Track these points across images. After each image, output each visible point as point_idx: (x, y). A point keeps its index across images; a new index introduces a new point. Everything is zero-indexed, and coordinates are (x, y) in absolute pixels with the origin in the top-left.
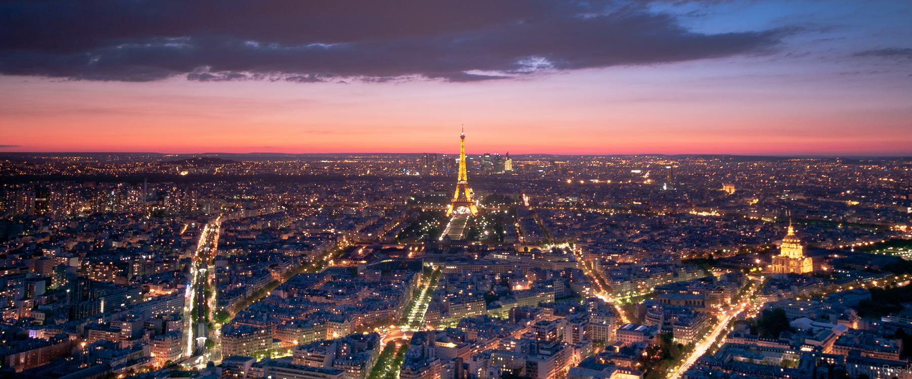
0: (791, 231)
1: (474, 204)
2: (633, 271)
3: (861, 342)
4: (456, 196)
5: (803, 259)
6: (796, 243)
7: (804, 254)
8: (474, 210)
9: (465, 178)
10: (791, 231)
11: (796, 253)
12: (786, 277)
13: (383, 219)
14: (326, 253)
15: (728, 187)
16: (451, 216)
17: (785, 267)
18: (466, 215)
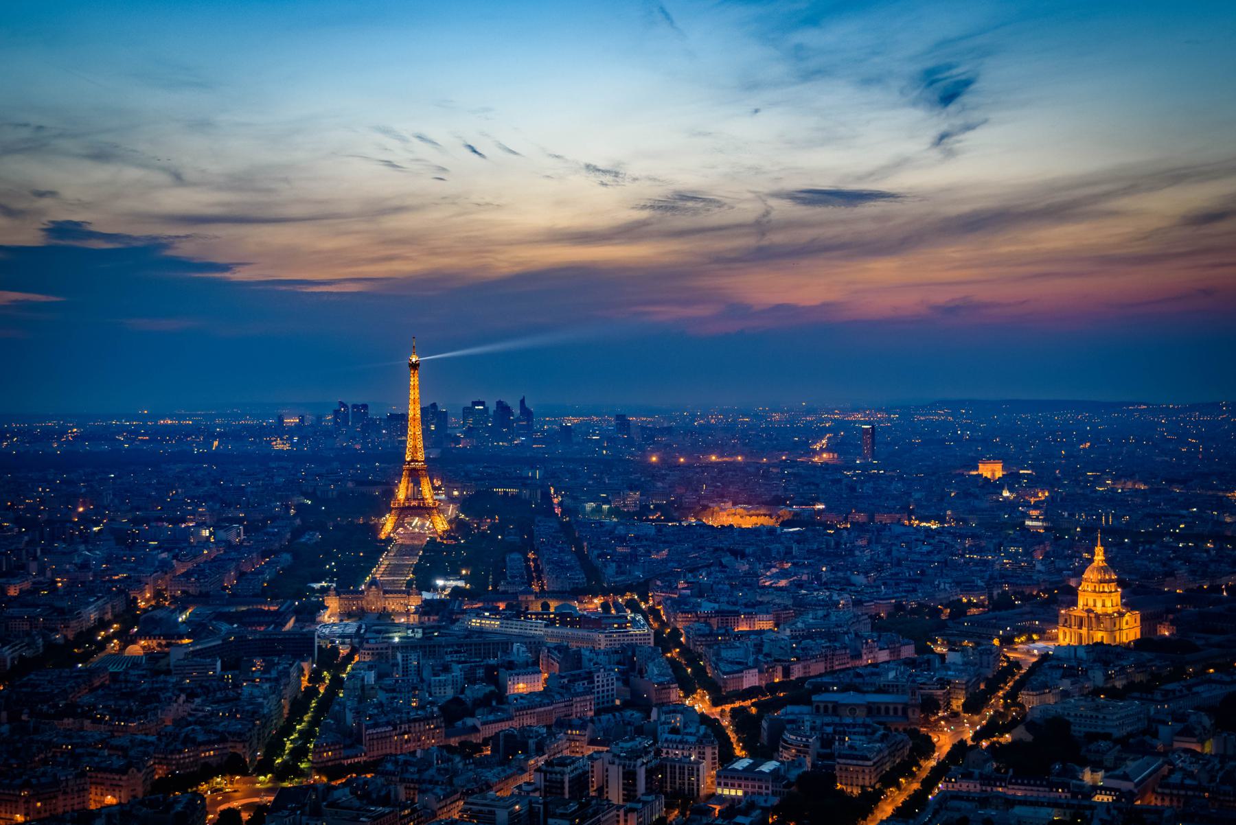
0: (1099, 556)
1: (440, 511)
2: (766, 650)
3: (1212, 779)
4: (402, 493)
5: (1121, 615)
6: (1110, 581)
7: (1124, 605)
8: (441, 524)
9: (421, 456)
10: (1099, 556)
11: (1108, 603)
12: (1082, 654)
13: (238, 548)
14: (103, 624)
15: (989, 466)
16: (389, 540)
17: (1084, 631)
18: (420, 536)
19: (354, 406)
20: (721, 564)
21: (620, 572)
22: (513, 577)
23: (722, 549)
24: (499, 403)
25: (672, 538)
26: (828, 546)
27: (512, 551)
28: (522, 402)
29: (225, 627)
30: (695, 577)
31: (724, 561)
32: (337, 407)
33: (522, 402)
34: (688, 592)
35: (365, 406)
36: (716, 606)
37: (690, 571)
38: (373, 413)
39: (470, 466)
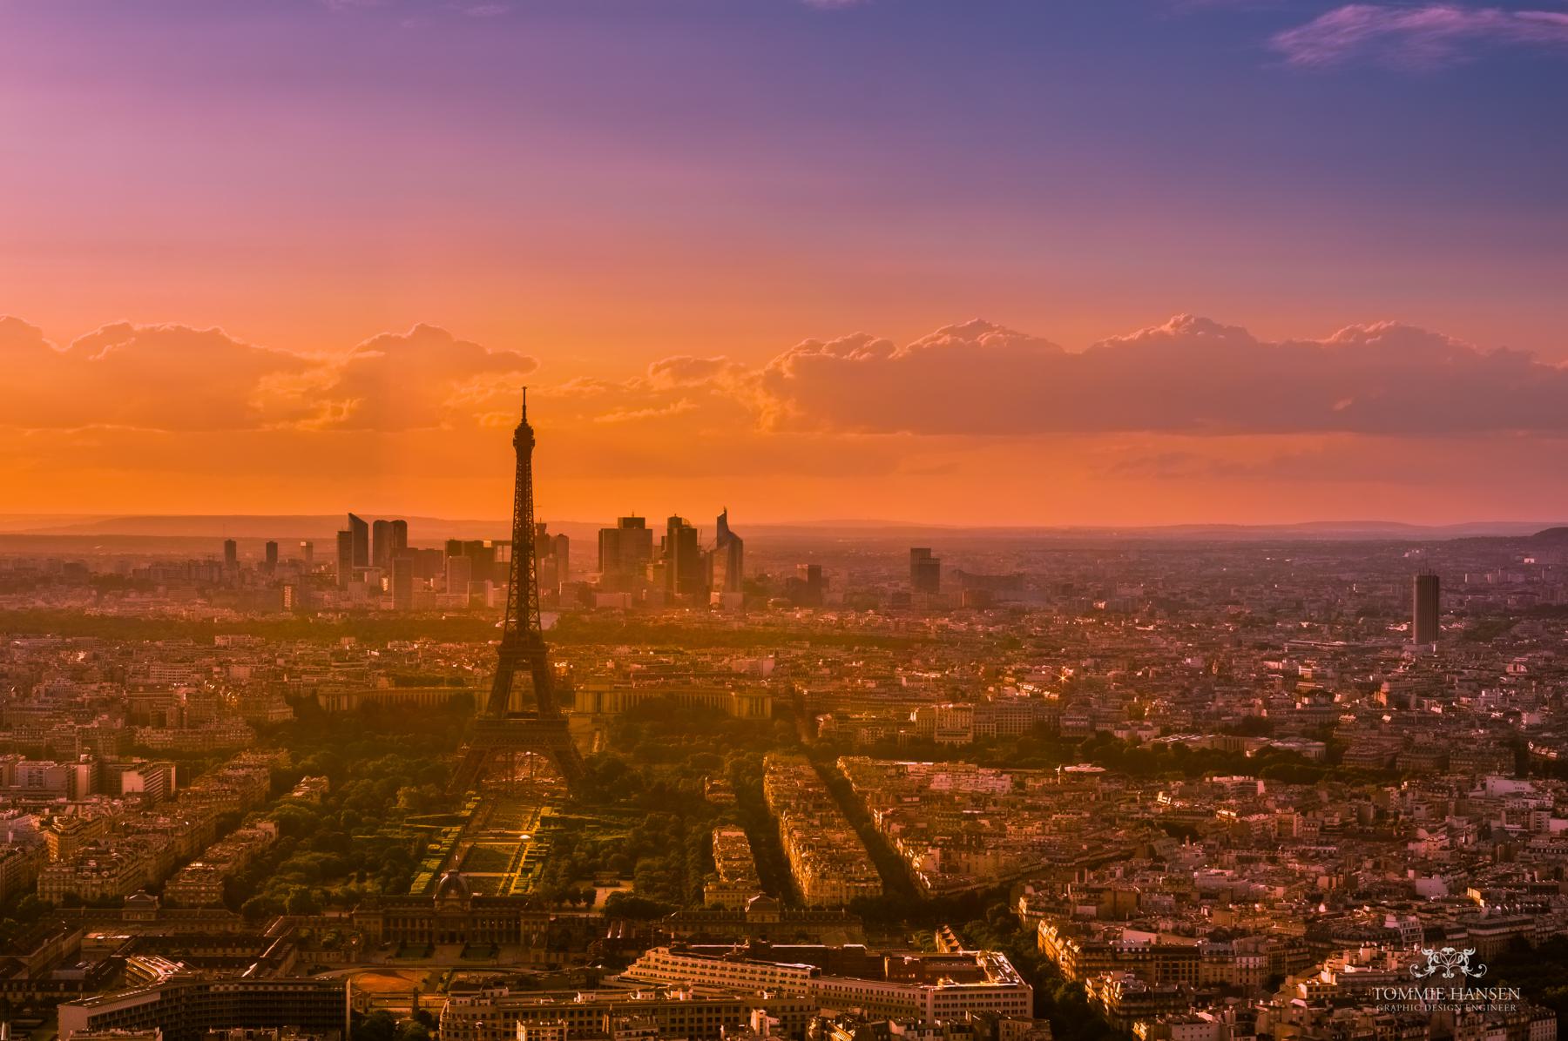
19: (380, 525)
20: (1151, 853)
21: (948, 866)
22: (731, 874)
23: (1150, 823)
24: (675, 522)
25: (1045, 801)
26: (1362, 819)
27: (724, 824)
28: (722, 520)
29: (162, 970)
30: (1101, 878)
31: (1159, 845)
32: (346, 527)
33: (722, 520)
34: (1092, 909)
35: (400, 526)
36: (1153, 937)
37: (1092, 868)
38: (414, 536)
39: (624, 650)
